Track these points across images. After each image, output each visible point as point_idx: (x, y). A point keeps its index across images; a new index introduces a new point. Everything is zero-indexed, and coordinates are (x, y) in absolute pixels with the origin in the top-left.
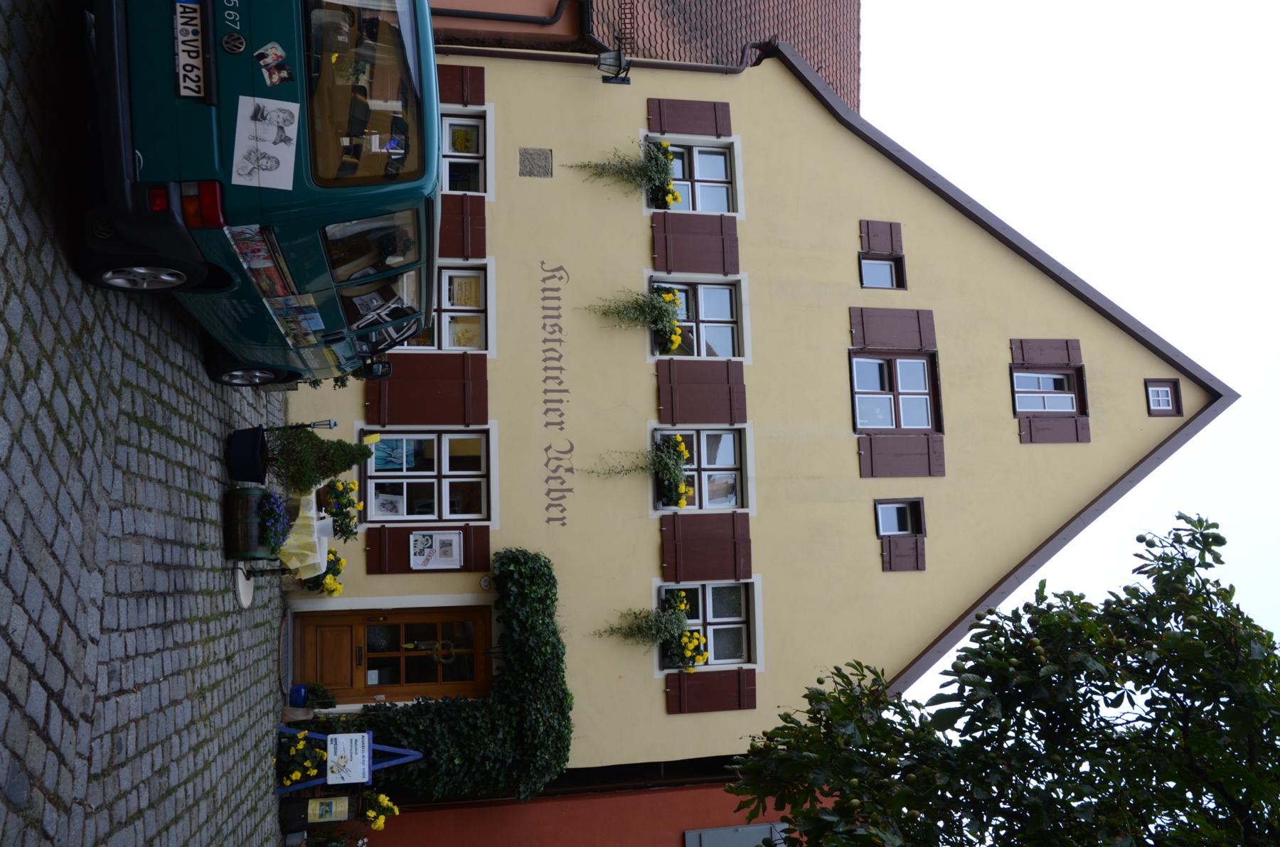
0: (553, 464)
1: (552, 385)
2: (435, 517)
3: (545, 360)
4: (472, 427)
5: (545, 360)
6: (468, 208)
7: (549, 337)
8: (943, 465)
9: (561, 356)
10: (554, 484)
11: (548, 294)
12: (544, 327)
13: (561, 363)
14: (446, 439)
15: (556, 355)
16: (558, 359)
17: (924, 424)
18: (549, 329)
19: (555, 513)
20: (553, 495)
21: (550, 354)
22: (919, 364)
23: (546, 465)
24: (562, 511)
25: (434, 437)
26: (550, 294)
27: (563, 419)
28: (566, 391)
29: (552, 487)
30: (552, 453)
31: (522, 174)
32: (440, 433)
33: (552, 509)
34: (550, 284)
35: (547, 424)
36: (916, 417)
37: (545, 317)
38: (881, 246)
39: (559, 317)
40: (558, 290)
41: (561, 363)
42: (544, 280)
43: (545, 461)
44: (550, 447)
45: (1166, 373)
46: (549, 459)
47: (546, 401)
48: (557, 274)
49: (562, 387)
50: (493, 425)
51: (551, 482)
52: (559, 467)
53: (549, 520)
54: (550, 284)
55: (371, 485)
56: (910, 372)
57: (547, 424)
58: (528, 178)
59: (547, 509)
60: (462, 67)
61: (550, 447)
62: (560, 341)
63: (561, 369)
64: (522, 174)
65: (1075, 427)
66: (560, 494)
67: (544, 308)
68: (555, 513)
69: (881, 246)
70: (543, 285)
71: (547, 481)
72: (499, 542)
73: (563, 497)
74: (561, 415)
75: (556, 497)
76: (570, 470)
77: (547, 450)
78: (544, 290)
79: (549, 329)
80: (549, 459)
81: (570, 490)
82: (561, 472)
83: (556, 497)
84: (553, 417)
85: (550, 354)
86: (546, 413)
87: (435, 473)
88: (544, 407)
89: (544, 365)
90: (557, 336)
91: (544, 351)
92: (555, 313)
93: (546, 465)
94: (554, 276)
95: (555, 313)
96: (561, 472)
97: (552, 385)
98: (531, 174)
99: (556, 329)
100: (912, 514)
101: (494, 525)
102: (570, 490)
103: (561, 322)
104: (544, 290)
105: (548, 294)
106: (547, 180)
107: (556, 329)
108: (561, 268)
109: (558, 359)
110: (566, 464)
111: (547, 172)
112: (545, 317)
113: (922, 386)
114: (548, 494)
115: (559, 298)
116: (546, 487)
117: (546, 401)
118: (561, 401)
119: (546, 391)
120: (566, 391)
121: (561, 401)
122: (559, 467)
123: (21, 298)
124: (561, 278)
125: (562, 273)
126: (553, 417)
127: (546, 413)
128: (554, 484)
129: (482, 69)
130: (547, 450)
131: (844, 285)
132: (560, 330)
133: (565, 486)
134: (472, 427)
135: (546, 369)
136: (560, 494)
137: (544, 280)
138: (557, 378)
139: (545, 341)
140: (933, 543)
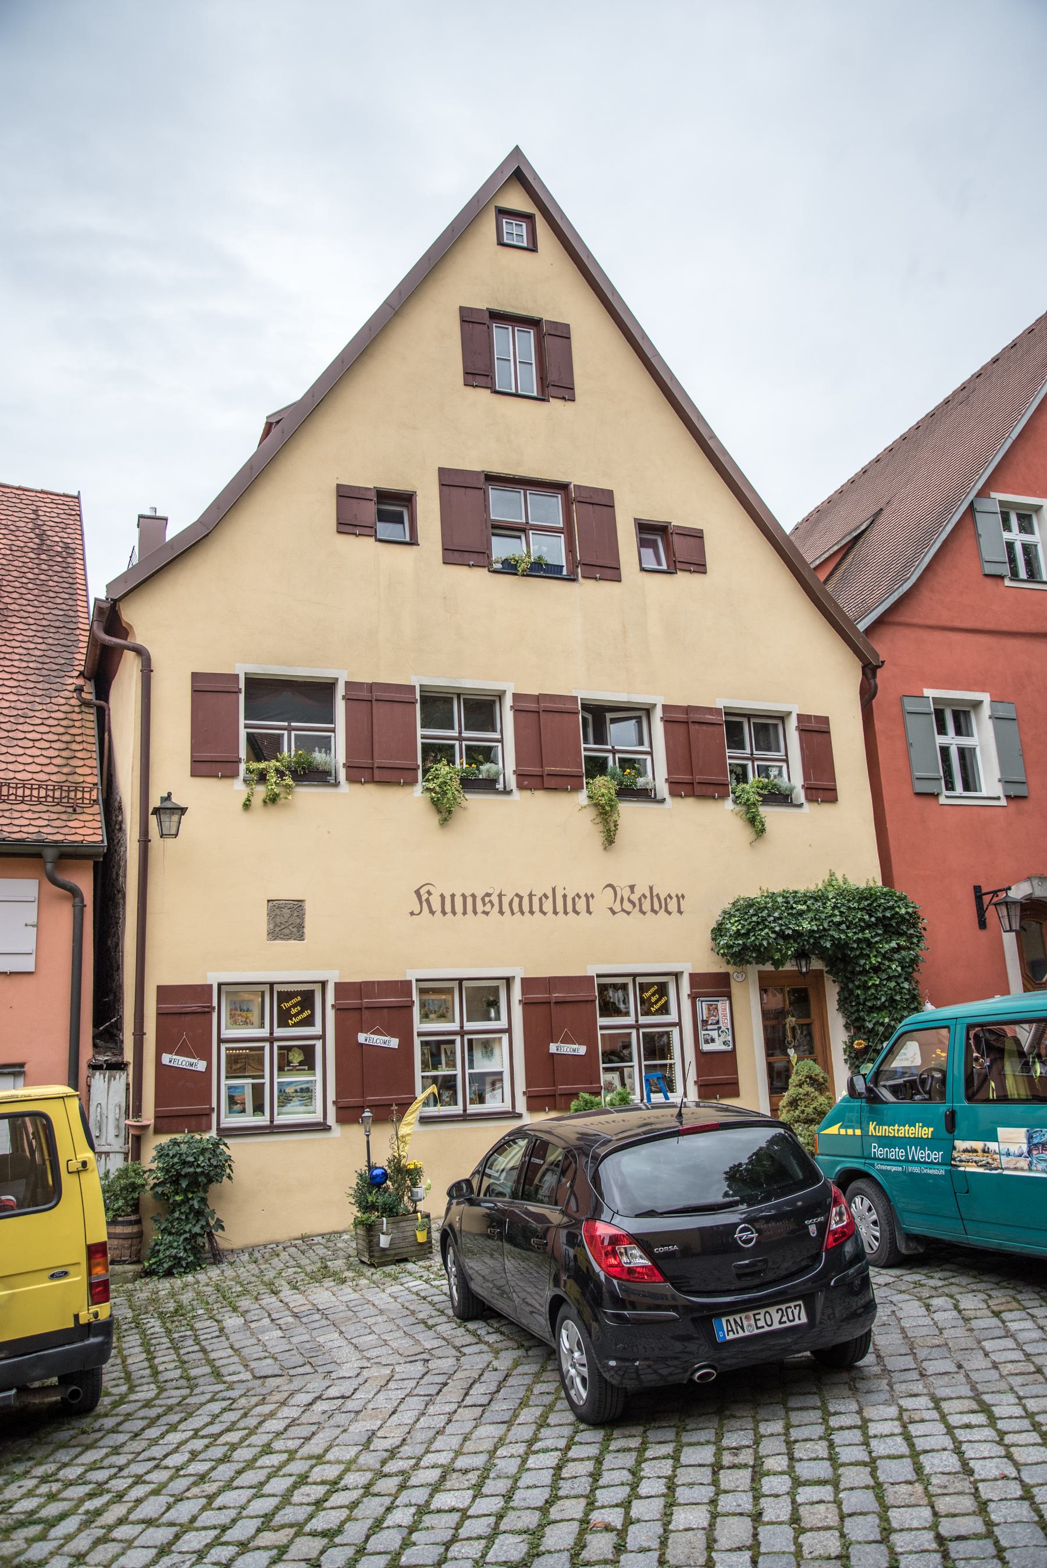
0: (627, 906)
1: (548, 906)
2: (676, 1031)
3: (523, 913)
4: (215, 1004)
5: (523, 913)
6: (353, 1002)
7: (496, 907)
8: (603, 491)
9: (517, 895)
10: (647, 906)
11: (448, 908)
12: (487, 913)
13: (525, 894)
14: (226, 1034)
15: (516, 900)
16: (521, 898)
17: (556, 503)
18: (488, 908)
19: (672, 906)
20: (656, 907)
21: (516, 908)
22: (494, 494)
23: (628, 913)
24: (671, 898)
25: (223, 1047)
26: (449, 906)
27: (582, 894)
28: (554, 890)
29: (649, 908)
30: (617, 907)
31: (301, 937)
32: (220, 1041)
33: (670, 909)
34: (436, 905)
35: (589, 912)
36: (550, 510)
37: (475, 912)
38: (377, 511)
39: (474, 896)
40: (442, 897)
41: (525, 894)
42: (432, 912)
43: (625, 915)
44: (611, 909)
45: (489, 224)
46: (623, 910)
47: (566, 913)
48: (424, 897)
49: (550, 894)
50: (213, 978)
51: (644, 909)
52: (630, 901)
53: (680, 912)
54: (436, 905)
55: (472, 1109)
56: (503, 506)
57: (589, 912)
58: (306, 930)
59: (670, 913)
60: (159, 1014)
61: (611, 909)
62: (500, 896)
63: (531, 895)
64: (301, 937)
65: (551, 340)
66: (655, 899)
67: (465, 913)
68: (672, 906)
69: (377, 511)
70: (439, 913)
71: (644, 913)
72: (708, 963)
73: (658, 895)
74: (578, 895)
75: (656, 903)
76: (632, 888)
77: (614, 913)
78: (444, 913)
79: (488, 908)
80: (623, 910)
81: (651, 888)
82: (635, 898)
83: (656, 903)
84: (581, 905)
85: (516, 908)
86: (578, 913)
87: (267, 1045)
88: (571, 914)
89: (527, 914)
90: (495, 899)
91: (513, 913)
92: (469, 900)
93: (628, 913)
94: (427, 900)
95: (469, 900)
96: (635, 898)
97: (548, 906)
98: (301, 927)
99: (487, 899)
100: (650, 532)
101: (687, 968)
102: (651, 888)
103: (479, 895)
104: (444, 913)
105: (448, 908)
106: (308, 906)
107: (487, 899)
108: (417, 893)
109: (521, 898)
110: (626, 893)
111: (298, 906)
112: (475, 912)
113: (516, 496)
114: (656, 912)
115: (453, 896)
116: (649, 914)
117: (566, 913)
118: (565, 896)
119: (555, 913)
120: (554, 890)
121: (565, 896)
122: (630, 901)
123: (110, 1528)
124: (429, 893)
125: (423, 891)
126: (581, 905)
127: (578, 913)
128: (647, 906)
129: (160, 988)
130: (614, 913)
131: (411, 569)
132: (488, 895)
133: (648, 894)
134: (215, 1004)
135: (532, 912)
136: (655, 899)
137: (432, 912)
138: (540, 899)
139: (501, 912)
140: (678, 519)
